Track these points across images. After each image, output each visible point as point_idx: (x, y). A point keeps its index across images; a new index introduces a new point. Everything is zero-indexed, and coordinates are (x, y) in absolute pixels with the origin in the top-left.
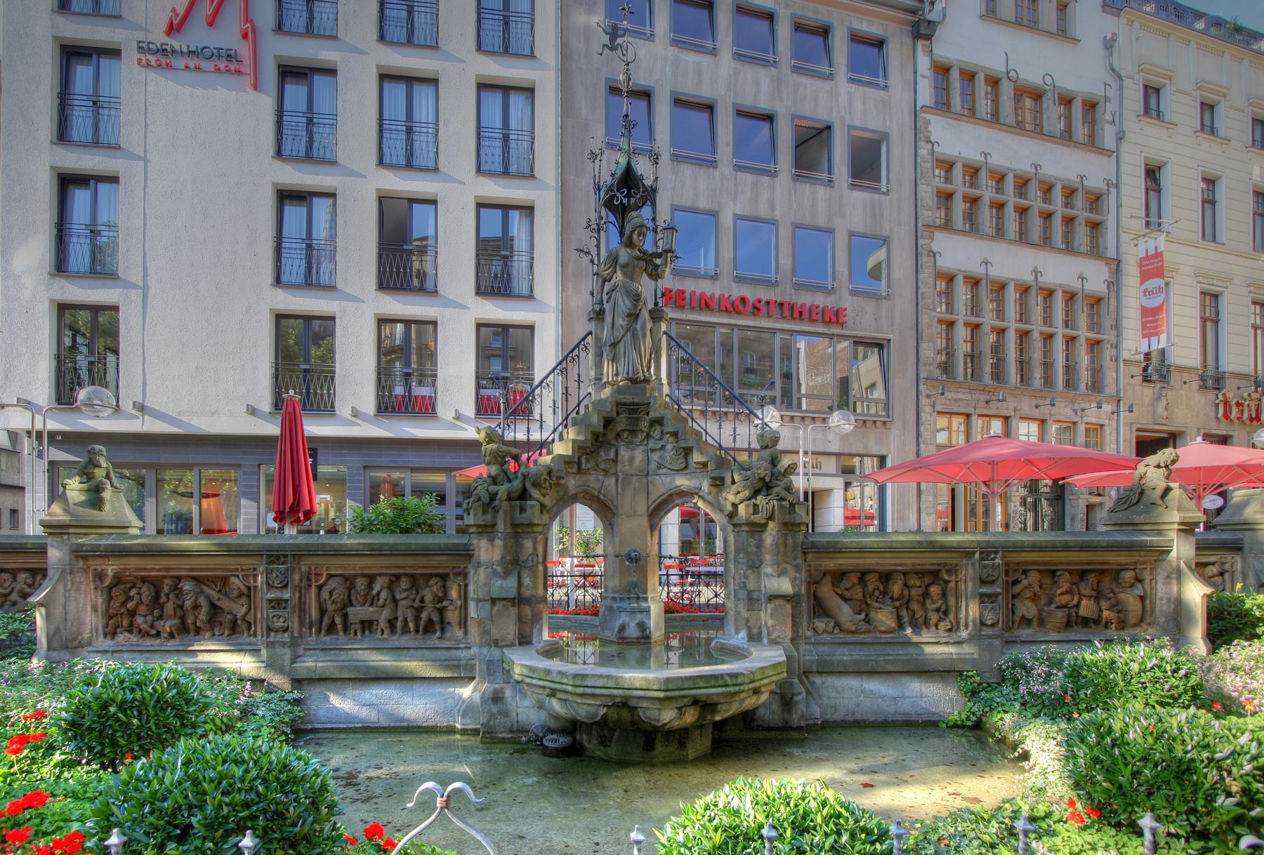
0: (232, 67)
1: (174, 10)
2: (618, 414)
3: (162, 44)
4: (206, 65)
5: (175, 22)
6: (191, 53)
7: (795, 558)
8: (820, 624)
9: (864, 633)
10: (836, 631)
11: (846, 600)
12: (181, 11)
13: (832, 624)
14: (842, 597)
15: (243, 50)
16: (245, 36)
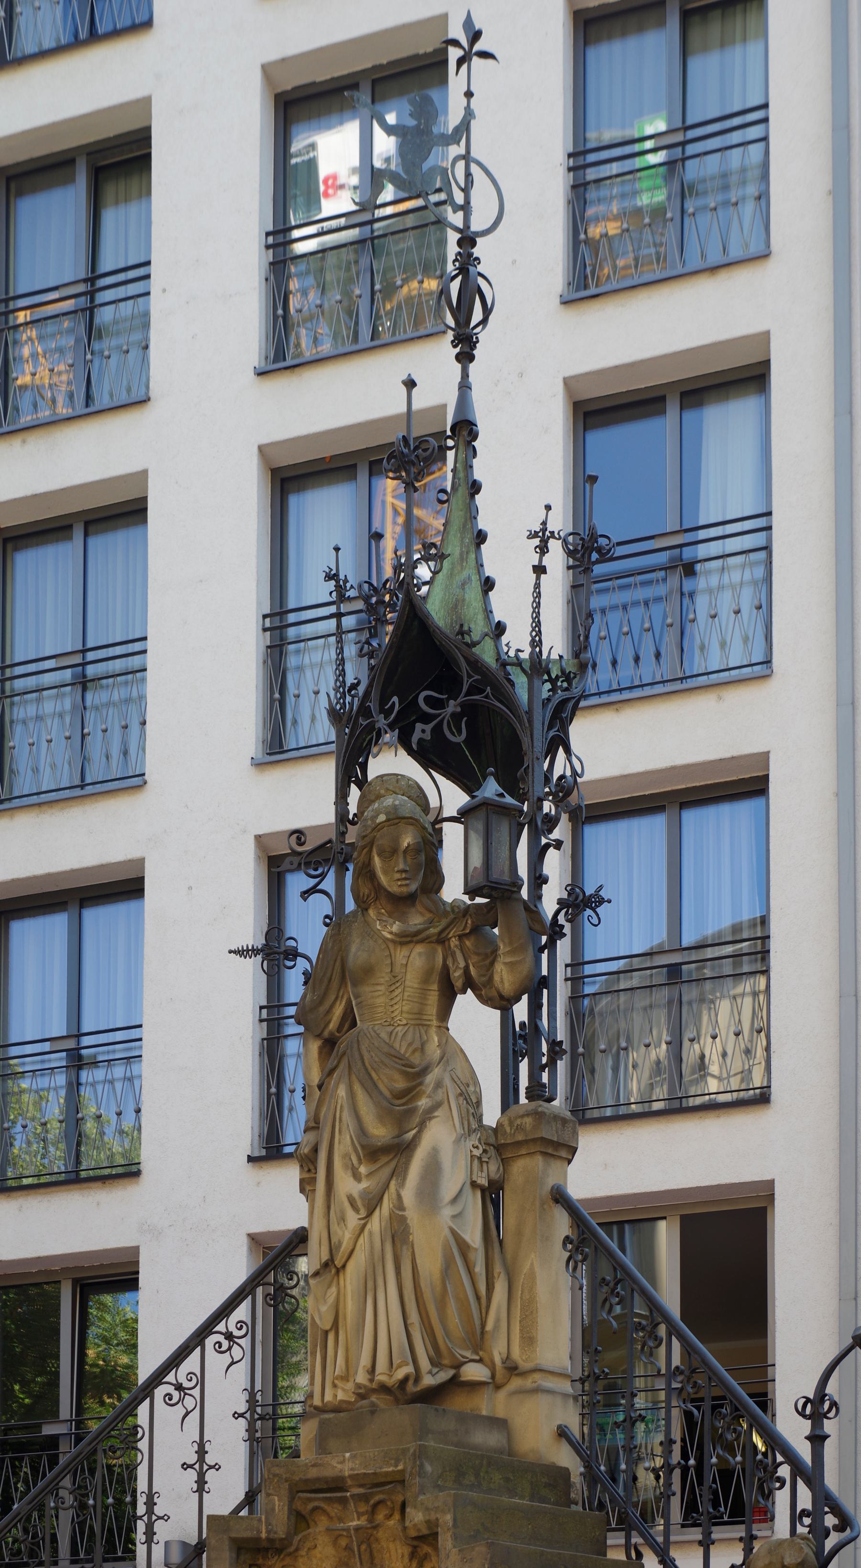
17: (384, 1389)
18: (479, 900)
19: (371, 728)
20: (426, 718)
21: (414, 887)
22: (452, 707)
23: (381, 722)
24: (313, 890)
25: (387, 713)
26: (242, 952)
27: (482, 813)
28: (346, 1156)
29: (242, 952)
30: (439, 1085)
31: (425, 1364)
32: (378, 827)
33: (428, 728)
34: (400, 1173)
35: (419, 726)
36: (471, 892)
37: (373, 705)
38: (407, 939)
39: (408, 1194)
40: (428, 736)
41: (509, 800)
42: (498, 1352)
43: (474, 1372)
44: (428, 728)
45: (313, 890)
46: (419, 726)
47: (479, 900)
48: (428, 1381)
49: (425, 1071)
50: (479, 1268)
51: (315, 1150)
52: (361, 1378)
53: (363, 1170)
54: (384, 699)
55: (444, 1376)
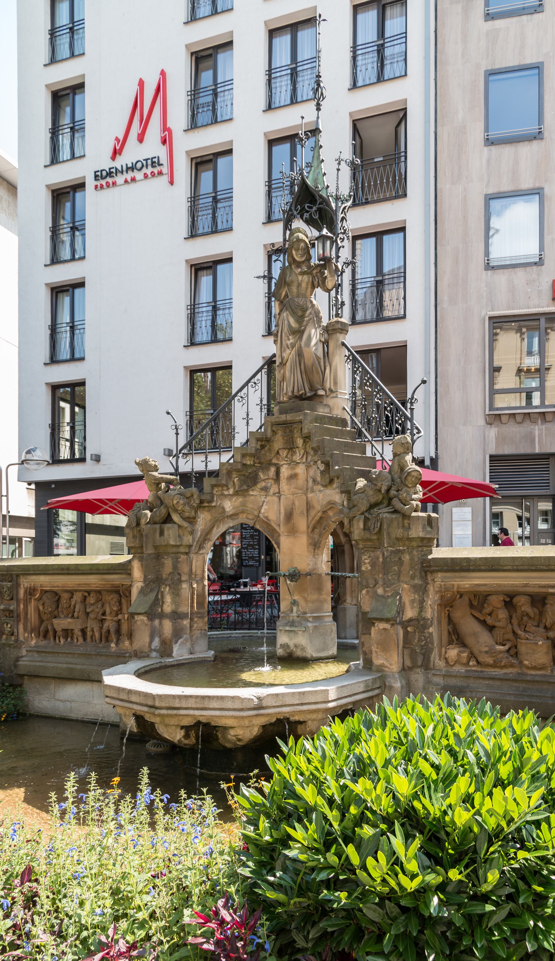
0: (156, 171)
1: (117, 139)
2: (274, 432)
3: (110, 169)
4: (139, 175)
5: (118, 148)
6: (128, 169)
7: (413, 578)
8: (453, 653)
9: (505, 667)
10: (471, 663)
11: (491, 629)
12: (121, 138)
13: (465, 655)
14: (483, 623)
15: (161, 152)
16: (164, 142)
17: (296, 397)
18: (321, 262)
19: (292, 214)
20: (307, 212)
21: (303, 259)
22: (315, 208)
23: (295, 213)
24: (277, 260)
25: (297, 210)
26: (258, 277)
27: (322, 238)
28: (286, 334)
29: (258, 277)
30: (310, 313)
31: (307, 390)
32: (294, 242)
33: (308, 214)
34: (301, 338)
35: (305, 214)
36: (319, 260)
37: (293, 208)
38: (303, 273)
39: (303, 344)
40: (308, 217)
41: (329, 234)
42: (328, 386)
43: (321, 392)
44: (308, 214)
45: (277, 260)
46: (305, 214)
47: (321, 262)
48: (309, 394)
49: (307, 310)
50: (322, 364)
51: (278, 332)
52: (290, 394)
53: (290, 337)
54: (296, 207)
55: (313, 393)
